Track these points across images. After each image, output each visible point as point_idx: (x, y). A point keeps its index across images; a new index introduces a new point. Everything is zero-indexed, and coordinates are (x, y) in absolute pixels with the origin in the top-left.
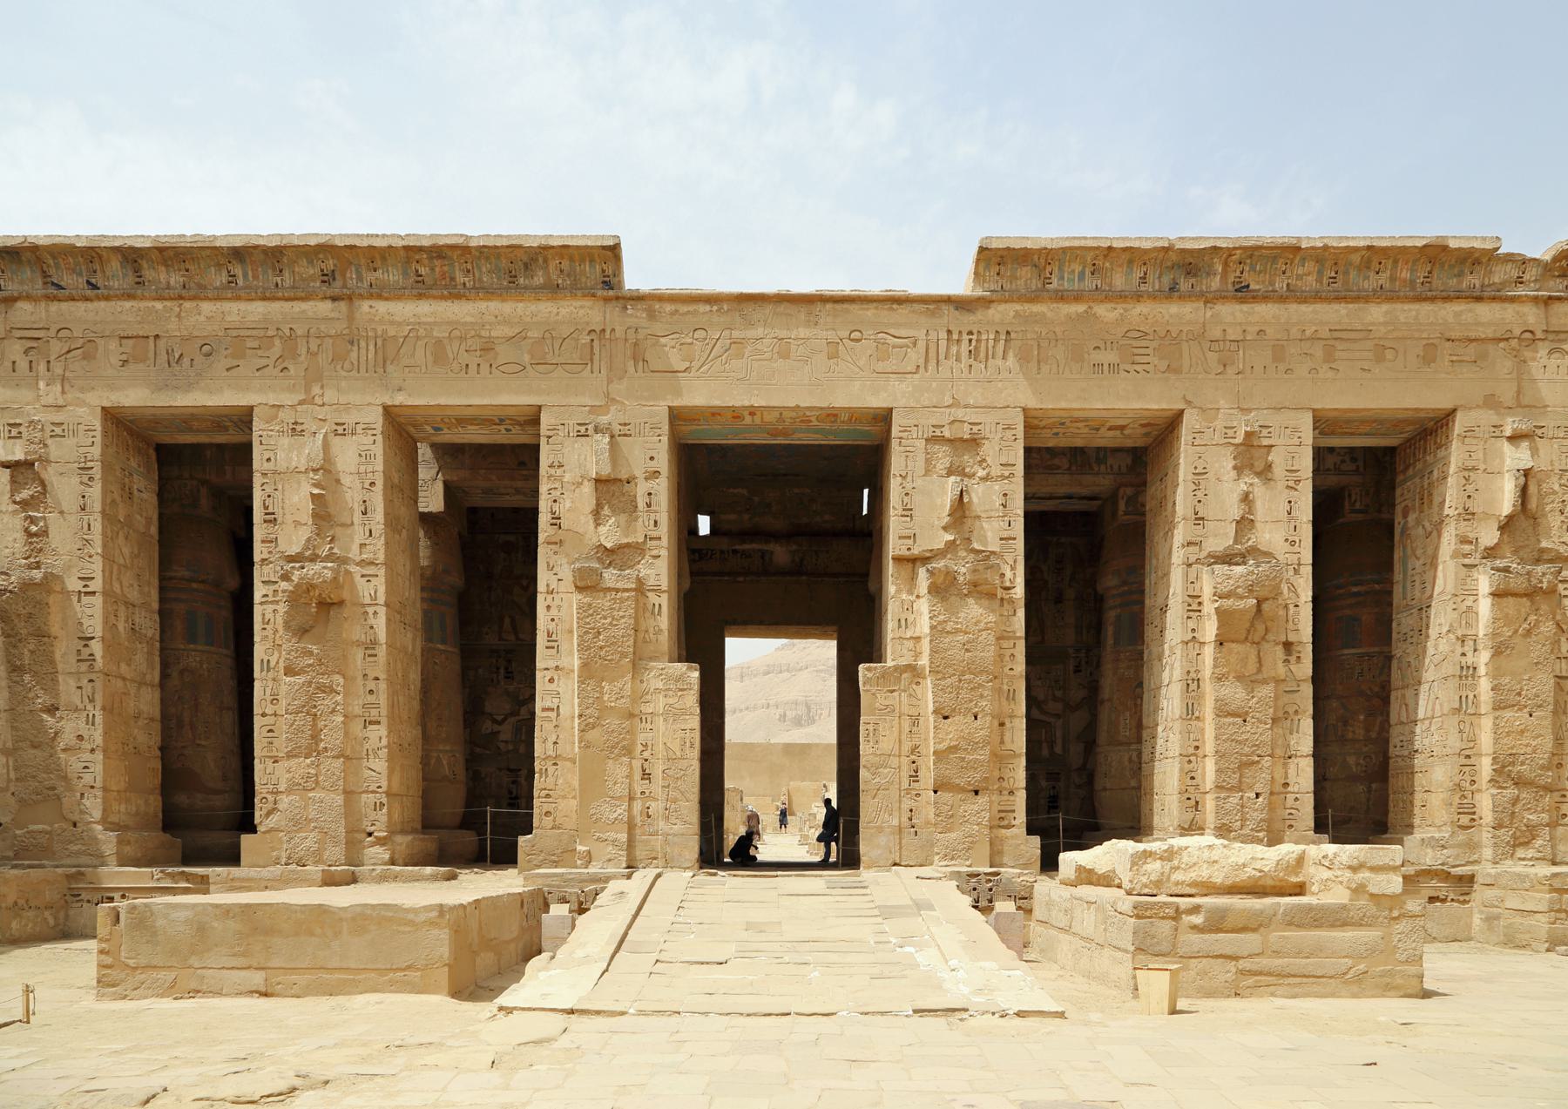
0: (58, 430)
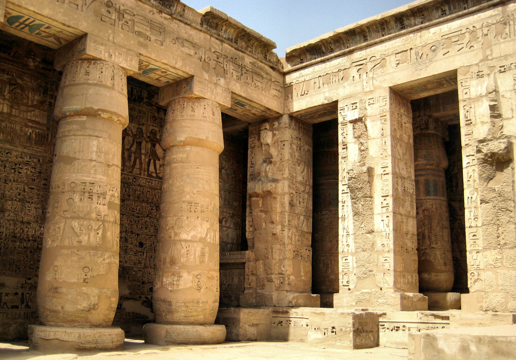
0: (371, 102)
